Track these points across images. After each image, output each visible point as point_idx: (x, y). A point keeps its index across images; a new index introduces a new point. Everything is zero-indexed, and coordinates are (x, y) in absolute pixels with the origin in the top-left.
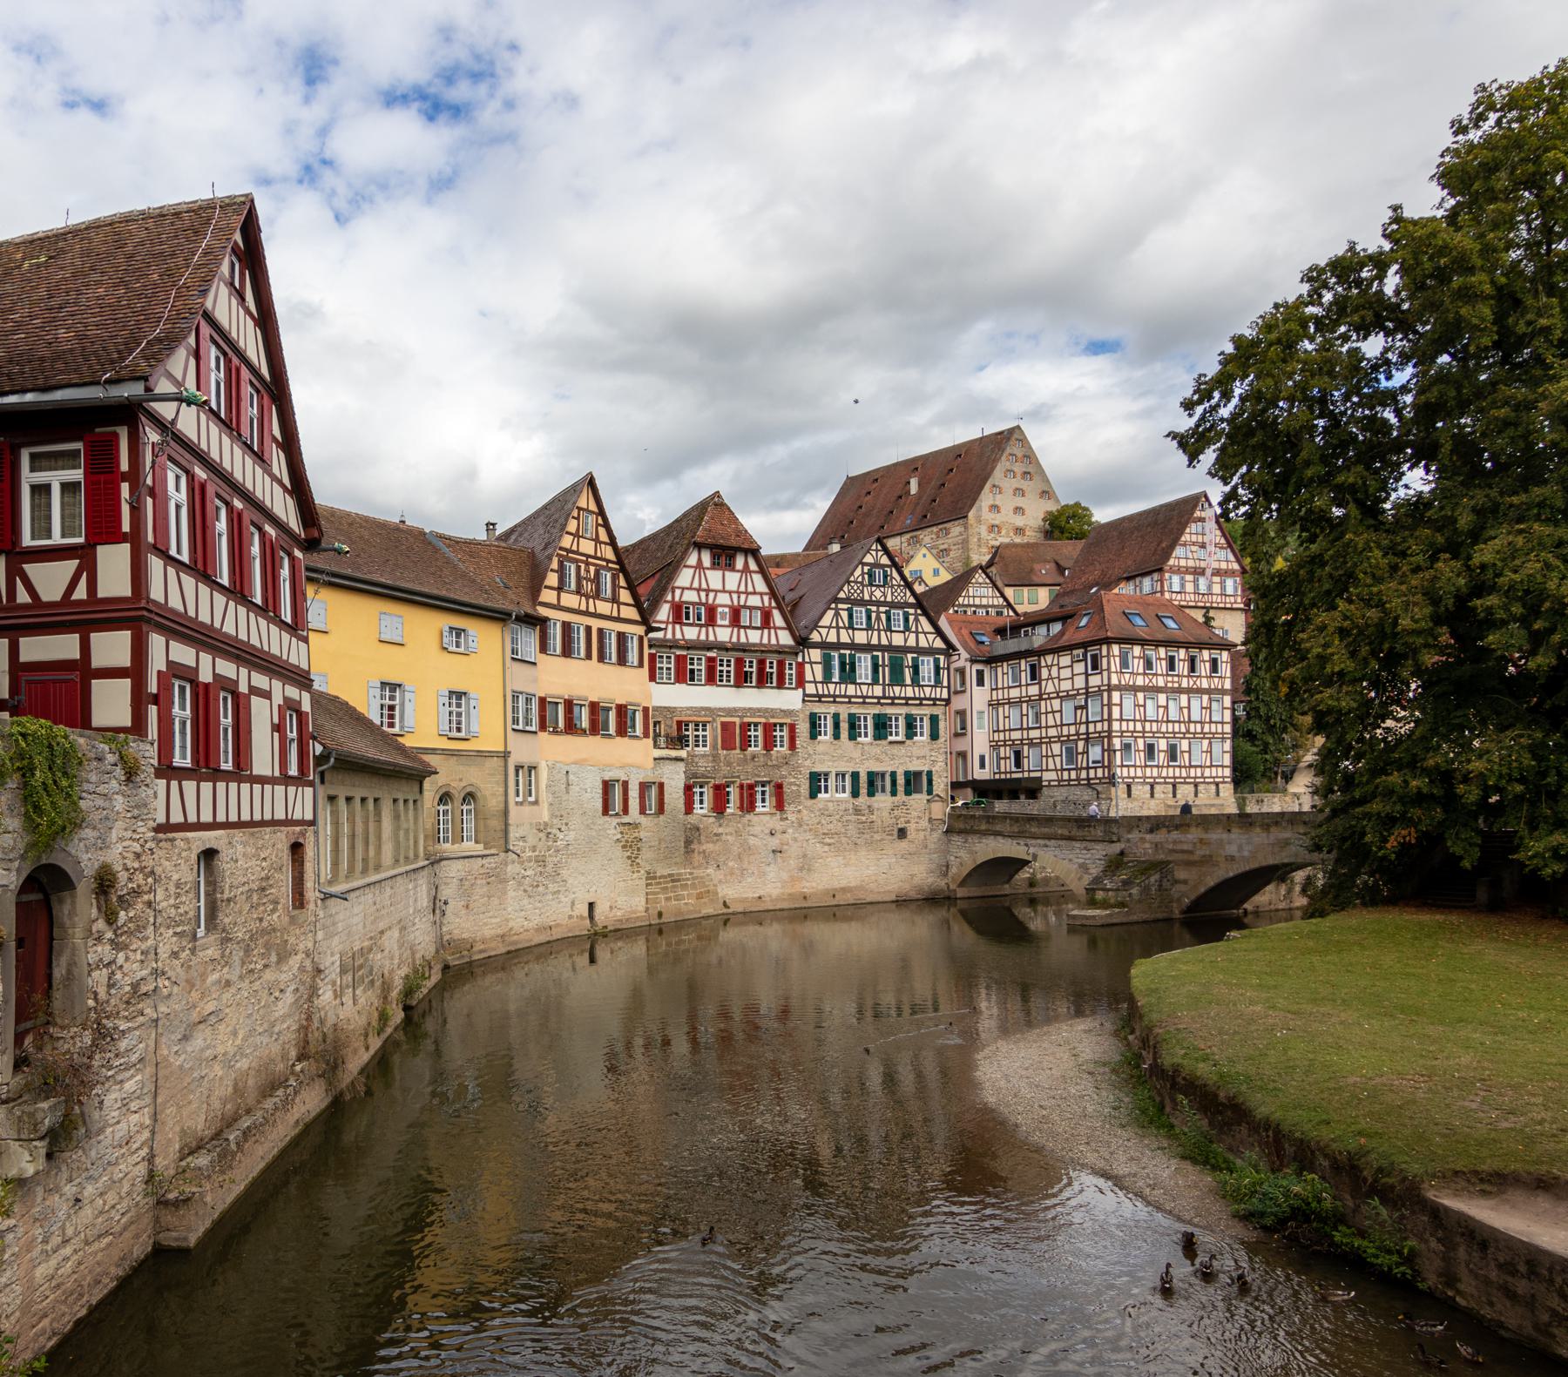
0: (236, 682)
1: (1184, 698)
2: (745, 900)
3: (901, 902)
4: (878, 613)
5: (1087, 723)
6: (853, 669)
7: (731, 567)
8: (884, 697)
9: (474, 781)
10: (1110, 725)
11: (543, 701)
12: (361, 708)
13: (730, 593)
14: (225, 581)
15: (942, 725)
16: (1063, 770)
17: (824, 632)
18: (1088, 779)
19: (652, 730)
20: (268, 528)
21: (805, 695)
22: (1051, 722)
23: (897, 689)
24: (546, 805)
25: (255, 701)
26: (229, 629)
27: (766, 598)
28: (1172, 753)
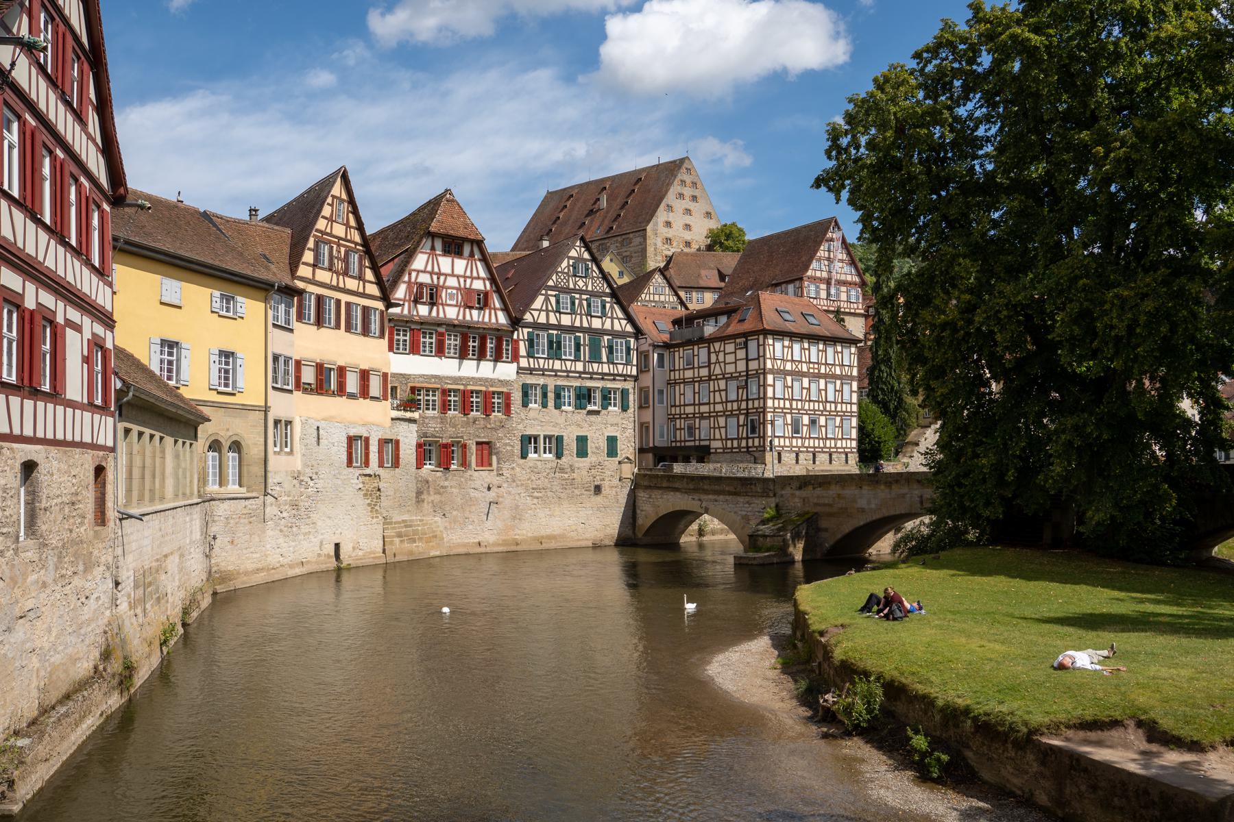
0: (54, 313)
2: (465, 545)
3: (596, 547)
4: (581, 300)
5: (747, 400)
6: (559, 347)
7: (459, 254)
8: (584, 373)
9: (239, 431)
10: (765, 403)
11: (298, 364)
12: (145, 361)
13: (458, 277)
14: (47, 220)
15: (631, 397)
16: (727, 439)
17: (536, 314)
18: (748, 447)
19: (389, 391)
20: (83, 179)
21: (519, 368)
22: (718, 399)
23: (595, 366)
24: (299, 456)
25: (69, 332)
26: (50, 263)
27: (488, 283)
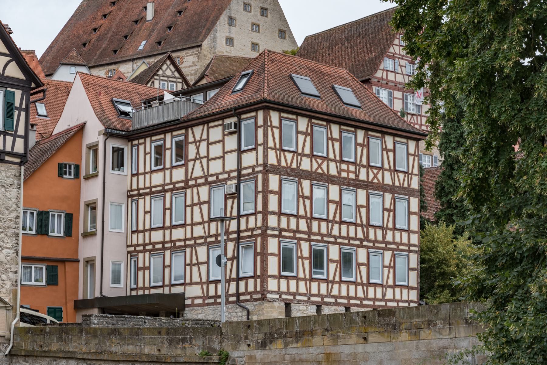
1: (362, 194)
5: (239, 216)
10: (265, 220)
18: (238, 295)
28: (346, 261)
